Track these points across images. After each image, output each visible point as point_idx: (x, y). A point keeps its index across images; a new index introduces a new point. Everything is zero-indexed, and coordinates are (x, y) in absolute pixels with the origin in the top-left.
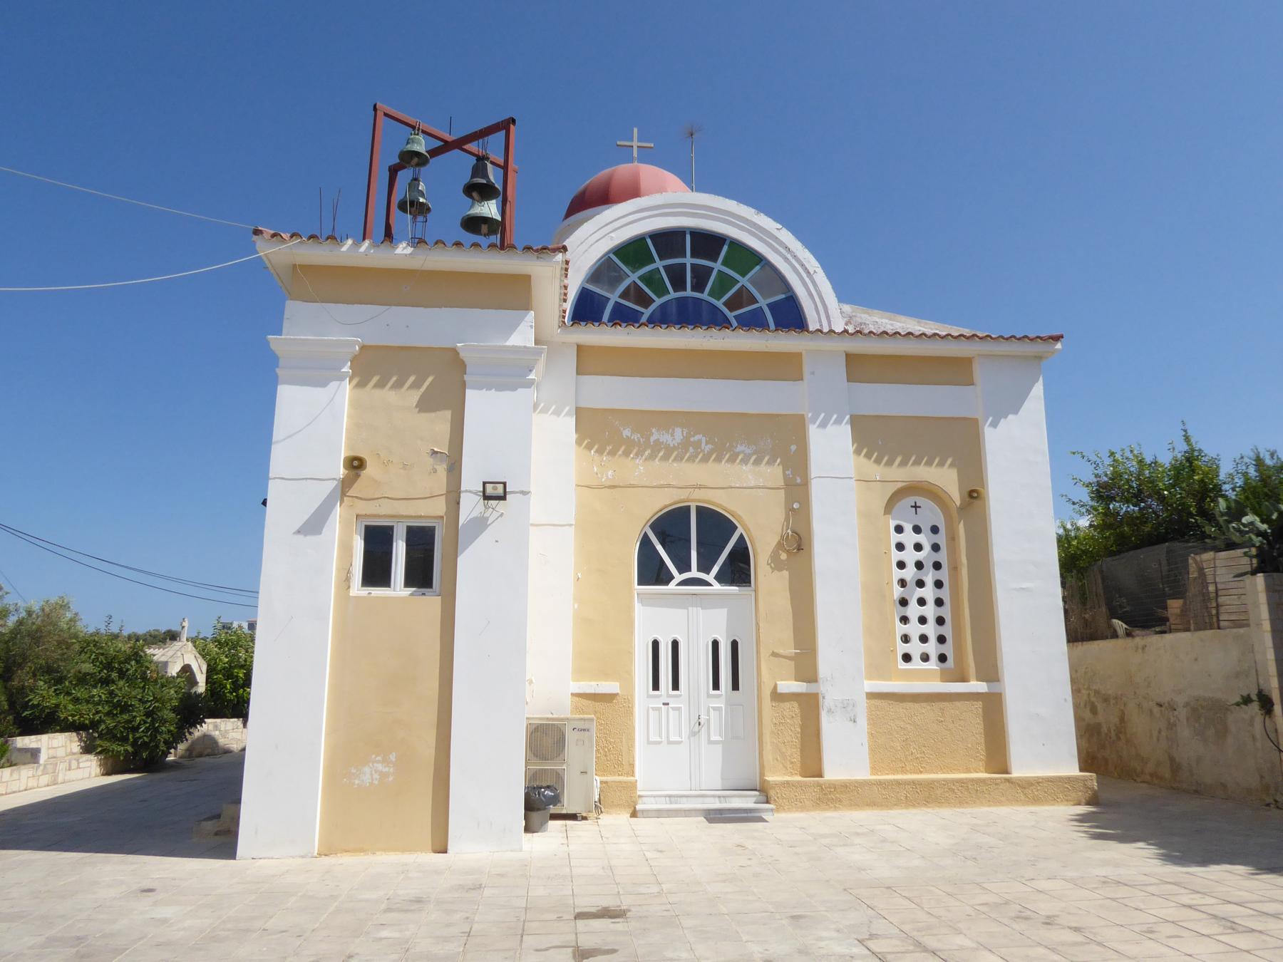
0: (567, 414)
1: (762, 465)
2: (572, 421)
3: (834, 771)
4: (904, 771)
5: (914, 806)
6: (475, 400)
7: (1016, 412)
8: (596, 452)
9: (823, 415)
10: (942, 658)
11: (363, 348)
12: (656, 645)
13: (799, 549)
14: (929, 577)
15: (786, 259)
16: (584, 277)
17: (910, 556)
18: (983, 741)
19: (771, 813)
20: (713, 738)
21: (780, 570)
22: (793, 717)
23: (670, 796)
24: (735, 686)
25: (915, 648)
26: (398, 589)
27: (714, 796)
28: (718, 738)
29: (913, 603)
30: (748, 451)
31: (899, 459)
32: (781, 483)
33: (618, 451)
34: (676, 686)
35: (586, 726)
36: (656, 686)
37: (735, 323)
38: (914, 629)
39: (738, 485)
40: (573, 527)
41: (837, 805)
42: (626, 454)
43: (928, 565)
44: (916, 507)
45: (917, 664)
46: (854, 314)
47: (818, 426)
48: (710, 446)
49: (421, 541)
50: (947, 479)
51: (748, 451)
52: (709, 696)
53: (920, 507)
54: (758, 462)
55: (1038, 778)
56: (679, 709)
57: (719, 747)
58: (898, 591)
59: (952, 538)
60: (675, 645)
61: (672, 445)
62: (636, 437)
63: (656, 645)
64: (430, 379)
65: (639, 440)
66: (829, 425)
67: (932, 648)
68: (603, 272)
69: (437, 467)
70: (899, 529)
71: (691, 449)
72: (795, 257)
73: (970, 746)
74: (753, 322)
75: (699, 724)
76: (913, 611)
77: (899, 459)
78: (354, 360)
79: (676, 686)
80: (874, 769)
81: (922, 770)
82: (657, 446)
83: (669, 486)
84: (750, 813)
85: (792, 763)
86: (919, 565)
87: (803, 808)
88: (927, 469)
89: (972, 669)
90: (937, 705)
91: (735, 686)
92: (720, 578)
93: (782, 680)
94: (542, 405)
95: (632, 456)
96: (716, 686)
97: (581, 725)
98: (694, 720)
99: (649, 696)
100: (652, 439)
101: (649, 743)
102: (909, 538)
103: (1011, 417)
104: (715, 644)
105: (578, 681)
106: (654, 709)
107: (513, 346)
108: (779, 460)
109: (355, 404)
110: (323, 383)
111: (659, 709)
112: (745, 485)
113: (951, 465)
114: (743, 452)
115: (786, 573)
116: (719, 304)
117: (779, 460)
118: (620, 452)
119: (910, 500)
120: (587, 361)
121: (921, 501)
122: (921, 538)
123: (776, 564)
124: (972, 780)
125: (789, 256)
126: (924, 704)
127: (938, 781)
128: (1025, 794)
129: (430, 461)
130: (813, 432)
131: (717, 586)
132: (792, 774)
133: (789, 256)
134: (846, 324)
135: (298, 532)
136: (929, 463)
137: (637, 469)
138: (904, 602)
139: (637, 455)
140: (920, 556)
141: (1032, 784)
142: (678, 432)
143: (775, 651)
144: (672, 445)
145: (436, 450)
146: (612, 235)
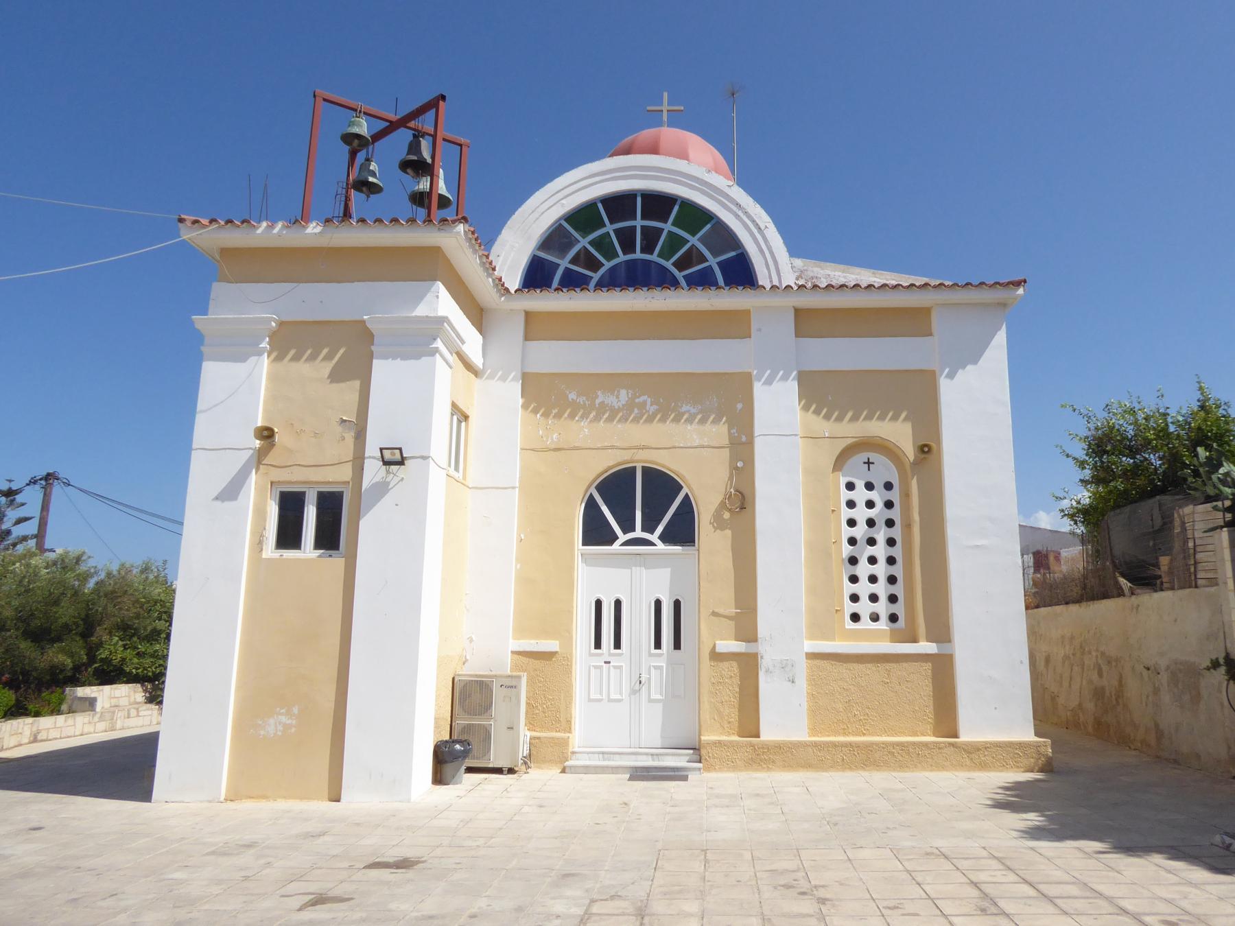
0: (513, 380)
1: (707, 425)
2: (518, 386)
3: (769, 733)
4: (845, 733)
5: (850, 769)
6: (380, 368)
7: (975, 361)
8: (542, 415)
9: (769, 372)
10: (893, 618)
11: (281, 324)
12: (599, 604)
13: (743, 508)
14: (881, 535)
15: (737, 216)
16: (535, 245)
17: (862, 514)
18: (931, 703)
19: (698, 772)
20: (654, 696)
21: (722, 529)
22: (731, 677)
23: (603, 753)
24: (677, 645)
25: (864, 608)
27: (647, 754)
28: (659, 697)
29: (863, 561)
30: (693, 411)
31: (850, 414)
32: (726, 441)
33: (563, 414)
34: (617, 645)
35: (514, 683)
36: (598, 645)
37: (683, 283)
38: (864, 589)
39: (682, 445)
40: (517, 489)
41: (770, 767)
42: (572, 416)
43: (881, 523)
44: (869, 463)
45: (866, 623)
46: (805, 268)
47: (764, 384)
48: (655, 407)
50: (900, 434)
51: (693, 411)
52: (650, 655)
53: (873, 463)
54: (703, 421)
55: (986, 743)
56: (620, 667)
57: (660, 706)
58: (847, 550)
59: (906, 495)
60: (618, 603)
61: (616, 407)
62: (581, 400)
63: (599, 604)
64: (342, 351)
65: (585, 404)
66: (775, 382)
67: (882, 608)
68: (555, 239)
69: (346, 435)
70: (851, 486)
71: (636, 411)
72: (746, 213)
73: (917, 708)
74: (703, 280)
75: (640, 683)
76: (863, 569)
77: (850, 414)
78: (273, 336)
79: (617, 645)
80: (814, 730)
81: (864, 732)
82: (602, 408)
83: (612, 447)
84: (678, 771)
85: (729, 722)
86: (871, 523)
87: (735, 768)
88: (880, 424)
89: (922, 629)
90: (882, 667)
91: (677, 645)
92: (665, 538)
93: (721, 640)
94: (489, 371)
95: (577, 418)
96: (658, 645)
97: (508, 682)
98: (635, 678)
99: (591, 655)
100: (597, 401)
101: (590, 700)
102: (861, 495)
103: (969, 367)
104: (658, 603)
105: (519, 639)
106: (595, 667)
108: (724, 419)
111: (600, 667)
112: (689, 445)
113: (906, 419)
114: (688, 411)
115: (728, 532)
116: (668, 265)
117: (724, 419)
118: (566, 415)
119: (863, 456)
120: (534, 326)
121: (873, 457)
122: (873, 495)
123: (719, 524)
124: (914, 744)
125: (740, 213)
126: (869, 666)
127: (877, 744)
128: (972, 759)
130: (758, 388)
131: (661, 546)
132: (729, 734)
133: (740, 213)
134: (797, 279)
136: (882, 418)
137: (582, 431)
138: (853, 561)
139: (582, 417)
140: (872, 513)
141: (979, 750)
142: (623, 392)
143: (716, 610)
144: (616, 407)
146: (563, 201)
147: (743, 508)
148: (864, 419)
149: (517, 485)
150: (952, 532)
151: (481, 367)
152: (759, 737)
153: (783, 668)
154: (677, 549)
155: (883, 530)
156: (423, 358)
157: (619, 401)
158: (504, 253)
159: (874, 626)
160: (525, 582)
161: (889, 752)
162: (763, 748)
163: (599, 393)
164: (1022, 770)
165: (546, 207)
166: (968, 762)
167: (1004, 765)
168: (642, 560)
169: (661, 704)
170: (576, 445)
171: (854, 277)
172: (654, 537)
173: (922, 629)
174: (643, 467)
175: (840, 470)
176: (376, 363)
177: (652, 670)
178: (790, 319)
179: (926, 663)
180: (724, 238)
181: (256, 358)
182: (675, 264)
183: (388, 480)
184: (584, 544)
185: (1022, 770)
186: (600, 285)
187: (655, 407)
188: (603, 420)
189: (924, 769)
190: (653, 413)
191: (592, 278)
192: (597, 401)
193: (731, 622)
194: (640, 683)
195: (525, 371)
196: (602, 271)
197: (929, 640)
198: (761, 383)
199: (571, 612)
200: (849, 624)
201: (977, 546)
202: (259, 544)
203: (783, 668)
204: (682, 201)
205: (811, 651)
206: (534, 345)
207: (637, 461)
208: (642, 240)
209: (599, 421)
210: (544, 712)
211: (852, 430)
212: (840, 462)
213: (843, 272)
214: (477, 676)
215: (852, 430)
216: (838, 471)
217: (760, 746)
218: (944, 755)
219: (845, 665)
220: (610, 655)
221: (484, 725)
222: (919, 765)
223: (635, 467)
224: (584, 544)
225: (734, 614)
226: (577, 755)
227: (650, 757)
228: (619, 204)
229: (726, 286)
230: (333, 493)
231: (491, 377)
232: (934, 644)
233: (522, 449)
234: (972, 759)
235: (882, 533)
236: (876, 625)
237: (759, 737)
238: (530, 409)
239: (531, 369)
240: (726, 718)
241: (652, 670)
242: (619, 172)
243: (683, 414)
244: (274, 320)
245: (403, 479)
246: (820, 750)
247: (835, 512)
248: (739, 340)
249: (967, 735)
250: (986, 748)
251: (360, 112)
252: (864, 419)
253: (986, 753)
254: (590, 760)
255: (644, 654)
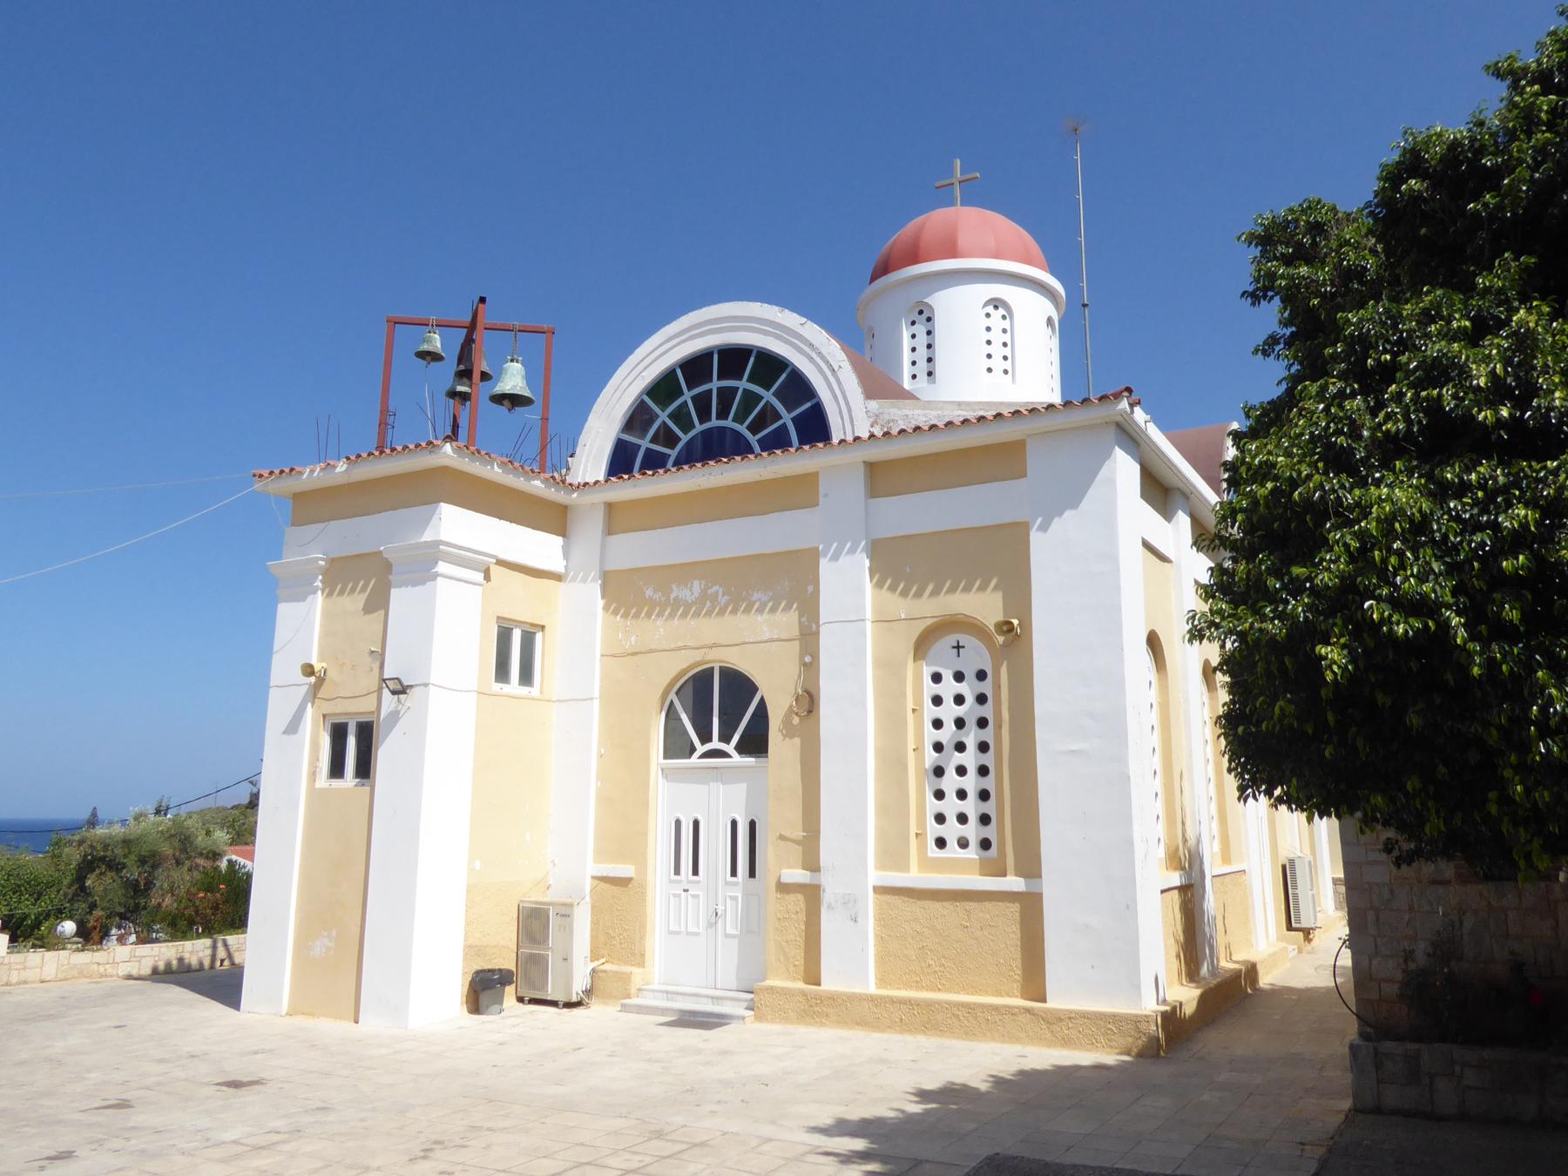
0: (594, 580)
1: (778, 613)
2: (596, 588)
3: (831, 982)
4: (918, 986)
5: (910, 1031)
6: (396, 595)
7: (1074, 503)
8: (622, 617)
9: (835, 545)
10: (985, 844)
11: (332, 561)
12: (678, 823)
13: (810, 712)
14: (971, 738)
15: (811, 359)
16: (619, 427)
17: (949, 712)
18: (1019, 955)
19: (741, 1022)
20: (730, 930)
21: (791, 737)
22: (797, 912)
23: (667, 992)
24: (752, 874)
25: (952, 830)
26: (348, 780)
27: (707, 996)
28: (734, 932)
29: (951, 772)
30: (765, 598)
31: (930, 588)
32: (796, 632)
33: (641, 614)
34: (695, 872)
35: (567, 912)
36: (677, 871)
37: (757, 449)
38: (951, 806)
39: (751, 640)
40: (596, 703)
41: (823, 1021)
42: (649, 615)
43: (971, 724)
44: (958, 647)
45: (953, 851)
46: (881, 411)
47: (830, 560)
48: (726, 597)
49: (366, 733)
50: (986, 606)
51: (765, 598)
52: (727, 883)
53: (963, 647)
54: (773, 610)
55: (1071, 1011)
56: (695, 896)
57: (735, 942)
58: (931, 757)
59: (997, 687)
60: (696, 824)
61: (690, 601)
62: (657, 596)
63: (678, 823)
64: (373, 582)
65: (661, 600)
66: (842, 557)
67: (972, 830)
68: (637, 419)
69: (373, 665)
70: (937, 678)
71: (708, 604)
72: (819, 354)
73: (1002, 961)
74: (777, 442)
75: (717, 914)
76: (951, 782)
77: (930, 588)
78: (326, 573)
79: (695, 872)
80: (882, 981)
81: (940, 987)
82: (677, 603)
83: (686, 648)
84: (723, 1019)
85: (795, 966)
86: (960, 723)
87: (786, 1020)
88: (965, 596)
89: (1010, 861)
90: (961, 906)
91: (752, 873)
92: (742, 749)
93: (789, 868)
94: (572, 573)
95: (653, 617)
96: (734, 873)
97: (563, 911)
98: (712, 911)
99: (671, 882)
100: (672, 597)
101: (670, 933)
102: (949, 688)
103: (1068, 514)
104: (734, 824)
105: (599, 863)
106: (675, 895)
107: (426, 542)
108: (795, 605)
109: (327, 614)
110: (303, 599)
111: (677, 896)
112: (759, 639)
113: (996, 588)
114: (759, 599)
115: (797, 741)
116: (742, 429)
117: (795, 605)
118: (643, 615)
119: (951, 639)
120: (616, 519)
121: (964, 639)
122: (963, 688)
123: (789, 731)
124: (982, 1006)
125: (814, 355)
126: (946, 904)
127: (939, 1003)
128: (1052, 1032)
129: (369, 659)
130: (824, 564)
131: (736, 758)
132: (794, 979)
133: (814, 355)
134: (872, 426)
135: (284, 732)
136: (967, 589)
137: (657, 630)
138: (939, 772)
139: (658, 616)
140: (960, 711)
141: (1061, 1020)
142: (696, 583)
143: (783, 833)
144: (690, 601)
145: (373, 649)
146: (643, 374)
147: (810, 712)
148: (947, 592)
149: (597, 694)
150: (1041, 734)
151: (563, 571)
152: (820, 985)
153: (845, 903)
154: (750, 760)
155: (973, 732)
156: (428, 583)
157: (693, 594)
158: (590, 442)
159: (962, 853)
160: (604, 800)
161: (953, 1014)
162: (816, 999)
163: (674, 587)
164: (1117, 1051)
165: (627, 384)
166: (1049, 1035)
167: (1093, 1044)
168: (720, 775)
169: (737, 940)
170: (653, 647)
171: (935, 413)
172: (730, 748)
173: (1010, 861)
174: (720, 667)
175: (923, 659)
176: (394, 591)
177: (728, 900)
178: (859, 477)
179: (1013, 903)
180: (798, 388)
181: (312, 596)
182: (749, 428)
183: (399, 708)
184: (666, 756)
185: (1117, 1051)
186: (678, 463)
187: (726, 597)
188: (677, 617)
189: (994, 1039)
190: (725, 604)
191: (670, 455)
192: (672, 597)
193: (798, 847)
194: (717, 914)
195: (607, 568)
196: (748, 434)
197: (1018, 874)
198: (827, 560)
199: (646, 834)
200: (933, 851)
201: (1073, 751)
202: (313, 775)
203: (845, 903)
204: (758, 352)
205: (879, 884)
206: (614, 539)
207: (714, 661)
208: (718, 404)
209: (674, 618)
210: (621, 944)
211: (932, 607)
212: (921, 647)
213: (924, 409)
214: (537, 903)
215: (932, 607)
216: (920, 659)
217: (813, 996)
218: (1019, 1023)
219: (918, 902)
220: (689, 882)
221: (543, 955)
222: (989, 1034)
223: (713, 668)
224: (666, 756)
225: (801, 838)
226: (644, 993)
227: (710, 1000)
228: (696, 367)
229: (762, 451)
230: (367, 722)
231: (574, 579)
232: (1022, 879)
233: (602, 656)
234: (1052, 1032)
235: (972, 735)
236: (965, 854)
237: (820, 985)
238: (611, 610)
239: (610, 567)
240: (792, 960)
241: (728, 900)
242: (705, 326)
243: (755, 602)
244: (322, 559)
245: (409, 708)
246: (876, 1006)
247: (916, 712)
248: (809, 509)
249: (1057, 1000)
250: (1070, 1018)
251: (432, 325)
252: (947, 592)
253: (1070, 1025)
254: (668, 999)
255: (721, 883)
